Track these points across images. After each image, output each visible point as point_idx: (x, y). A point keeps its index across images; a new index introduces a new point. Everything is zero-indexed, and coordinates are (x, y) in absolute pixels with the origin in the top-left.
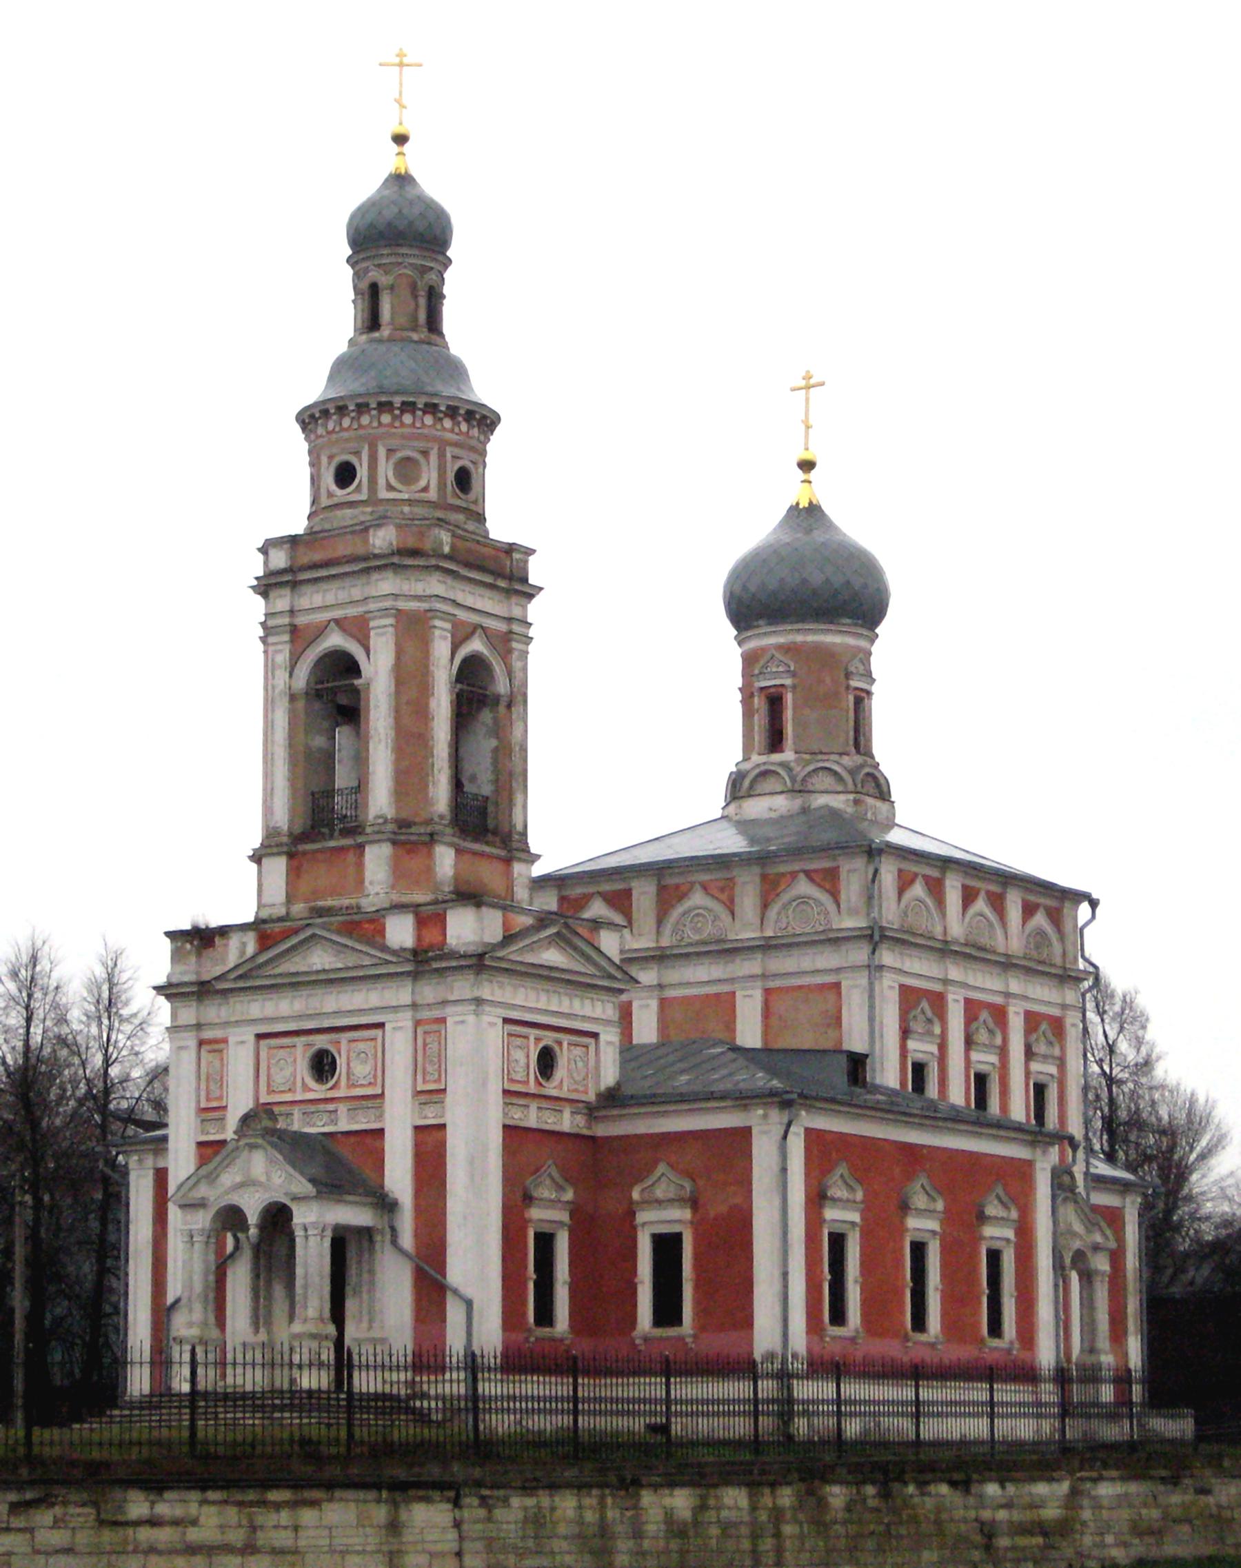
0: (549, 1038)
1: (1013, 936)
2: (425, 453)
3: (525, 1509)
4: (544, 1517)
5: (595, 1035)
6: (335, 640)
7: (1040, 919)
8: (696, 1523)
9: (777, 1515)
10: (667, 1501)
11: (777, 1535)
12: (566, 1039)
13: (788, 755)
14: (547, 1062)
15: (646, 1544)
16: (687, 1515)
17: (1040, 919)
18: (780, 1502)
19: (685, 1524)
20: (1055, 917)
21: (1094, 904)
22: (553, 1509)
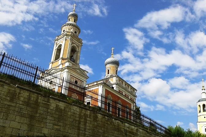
0: (77, 80)
1: (130, 90)
2: (72, 29)
3: (10, 90)
4: (16, 94)
5: (83, 82)
6: (61, 43)
7: (132, 90)
8: (64, 110)
9: (86, 115)
10: (58, 103)
11: (86, 120)
12: (79, 81)
13: (110, 74)
14: (76, 82)
15: (49, 110)
16: (63, 108)
17: (132, 90)
18: (87, 113)
19: (61, 109)
20: (133, 90)
21: (137, 91)
22: (19, 93)
